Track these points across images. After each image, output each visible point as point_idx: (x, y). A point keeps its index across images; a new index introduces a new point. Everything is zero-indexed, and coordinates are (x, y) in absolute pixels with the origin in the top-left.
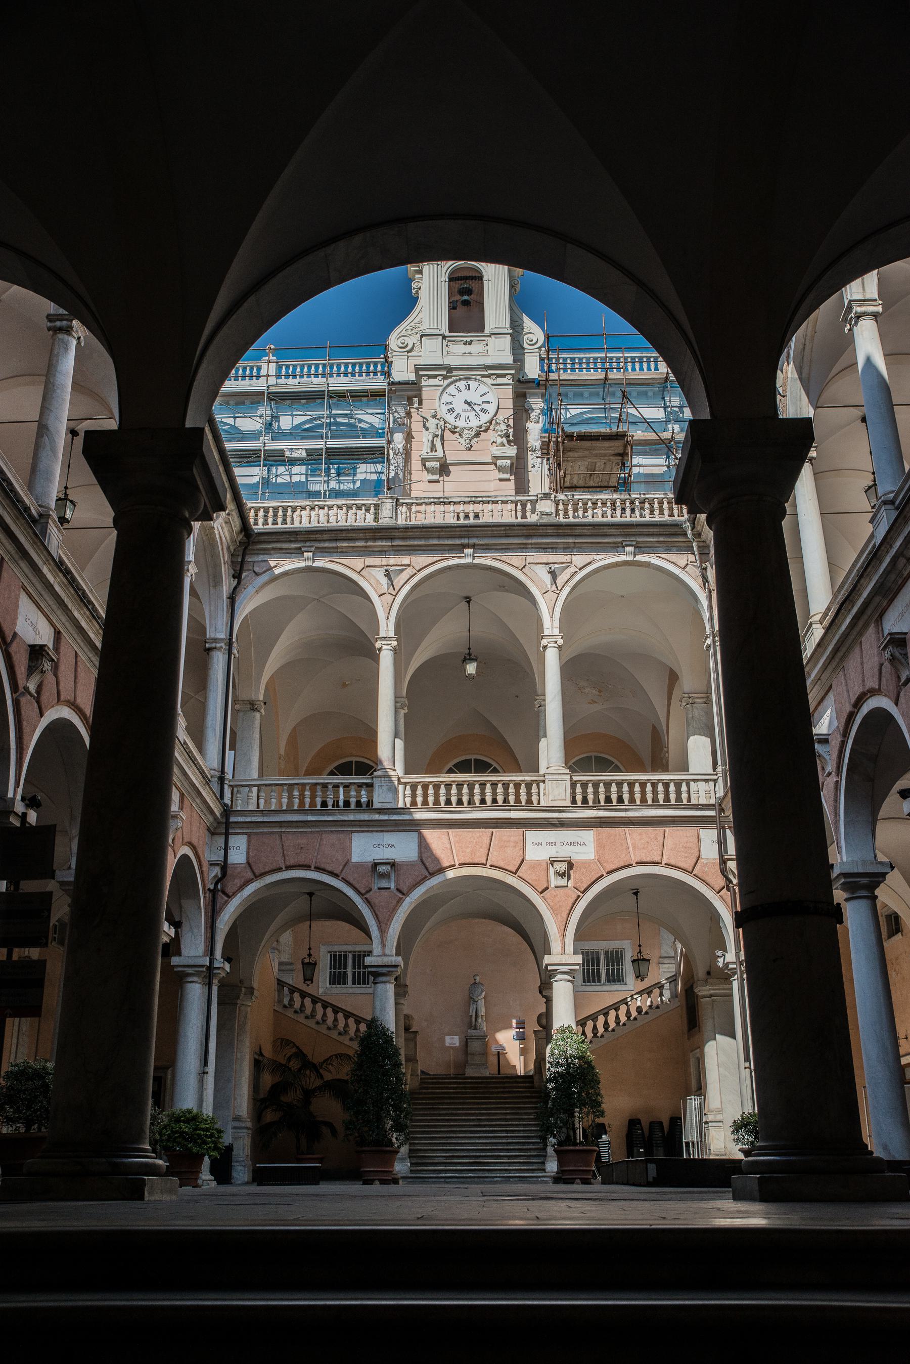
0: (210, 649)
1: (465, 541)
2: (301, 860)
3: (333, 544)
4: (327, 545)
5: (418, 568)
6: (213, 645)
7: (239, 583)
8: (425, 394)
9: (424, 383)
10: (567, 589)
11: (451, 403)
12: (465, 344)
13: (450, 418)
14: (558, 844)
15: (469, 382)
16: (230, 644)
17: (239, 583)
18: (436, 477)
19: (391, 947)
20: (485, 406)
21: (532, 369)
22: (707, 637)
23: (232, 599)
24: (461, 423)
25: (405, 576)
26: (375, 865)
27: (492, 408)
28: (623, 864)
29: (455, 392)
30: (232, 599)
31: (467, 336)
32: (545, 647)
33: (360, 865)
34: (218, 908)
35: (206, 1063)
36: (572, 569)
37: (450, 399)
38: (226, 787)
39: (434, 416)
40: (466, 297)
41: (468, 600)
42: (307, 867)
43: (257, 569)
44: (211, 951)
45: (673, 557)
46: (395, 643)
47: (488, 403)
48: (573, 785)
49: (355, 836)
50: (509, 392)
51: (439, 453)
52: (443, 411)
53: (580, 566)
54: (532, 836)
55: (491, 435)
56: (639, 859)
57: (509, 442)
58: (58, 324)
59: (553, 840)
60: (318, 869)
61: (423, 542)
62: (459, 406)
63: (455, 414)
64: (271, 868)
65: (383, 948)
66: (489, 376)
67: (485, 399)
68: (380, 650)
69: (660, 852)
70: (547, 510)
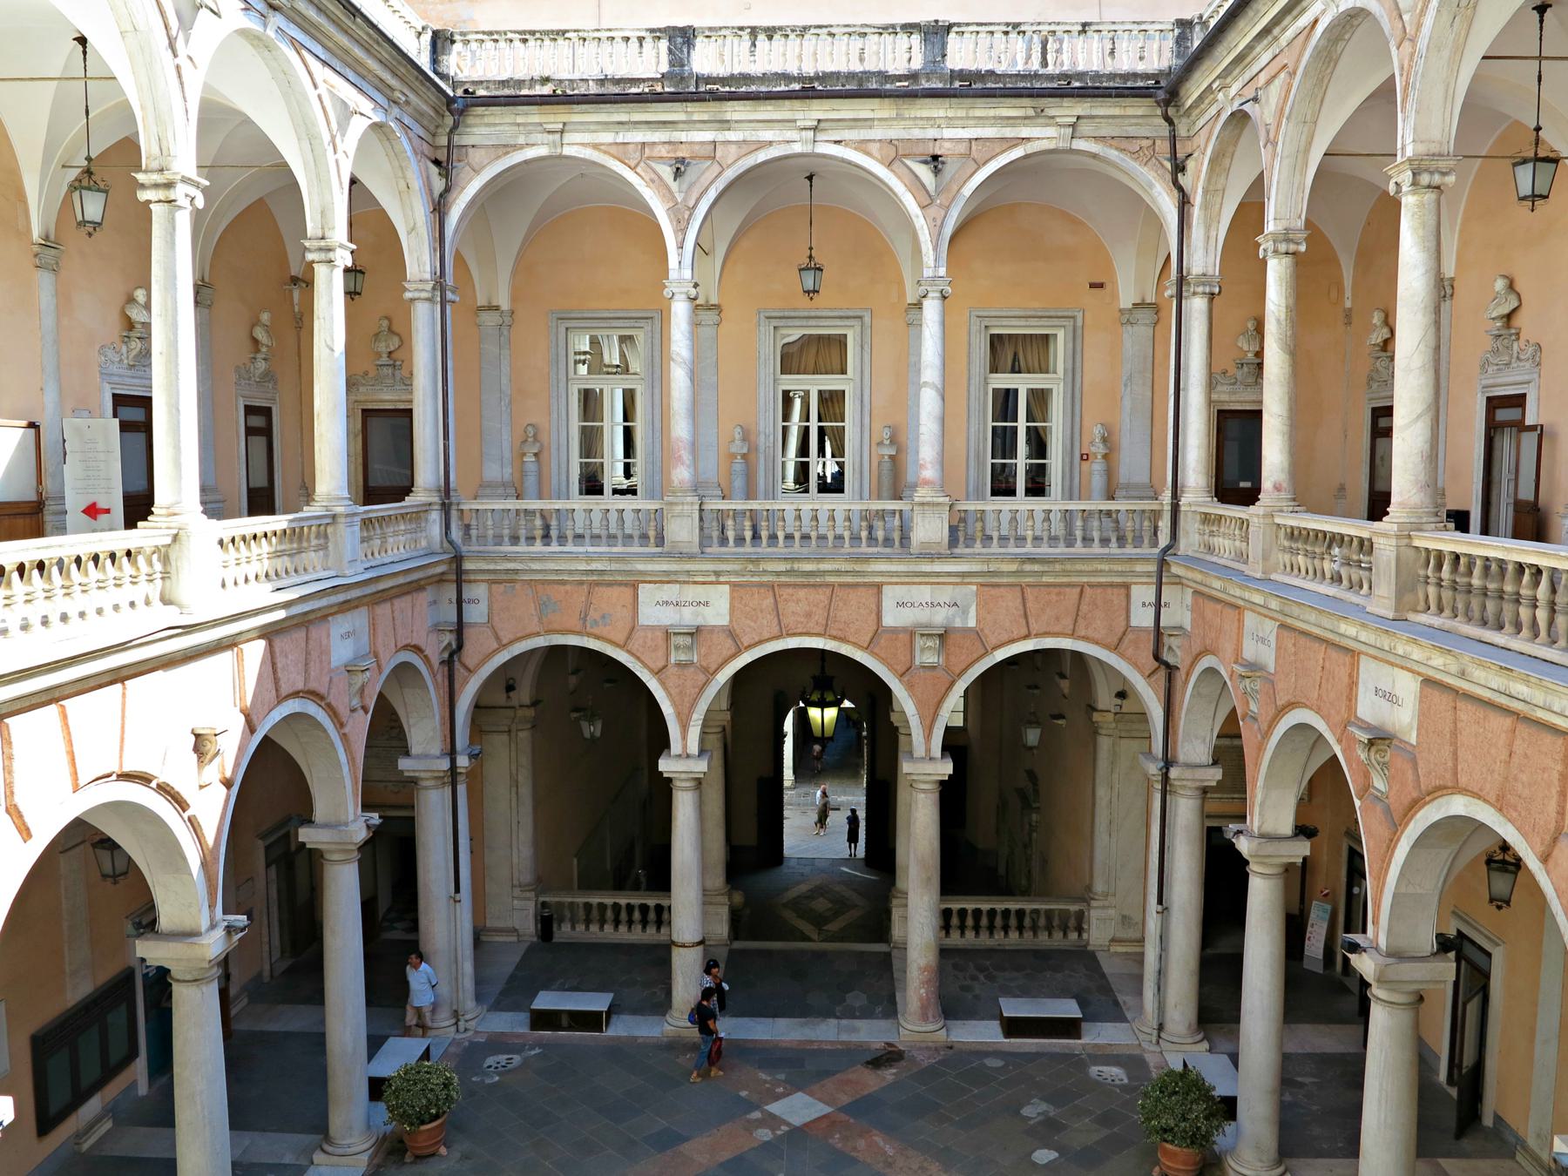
0: (412, 300)
6: (417, 295)
7: (447, 190)
17: (447, 190)
19: (693, 747)
23: (439, 208)
26: (668, 635)
30: (439, 208)
34: (457, 686)
35: (457, 890)
44: (452, 753)
65: (685, 747)
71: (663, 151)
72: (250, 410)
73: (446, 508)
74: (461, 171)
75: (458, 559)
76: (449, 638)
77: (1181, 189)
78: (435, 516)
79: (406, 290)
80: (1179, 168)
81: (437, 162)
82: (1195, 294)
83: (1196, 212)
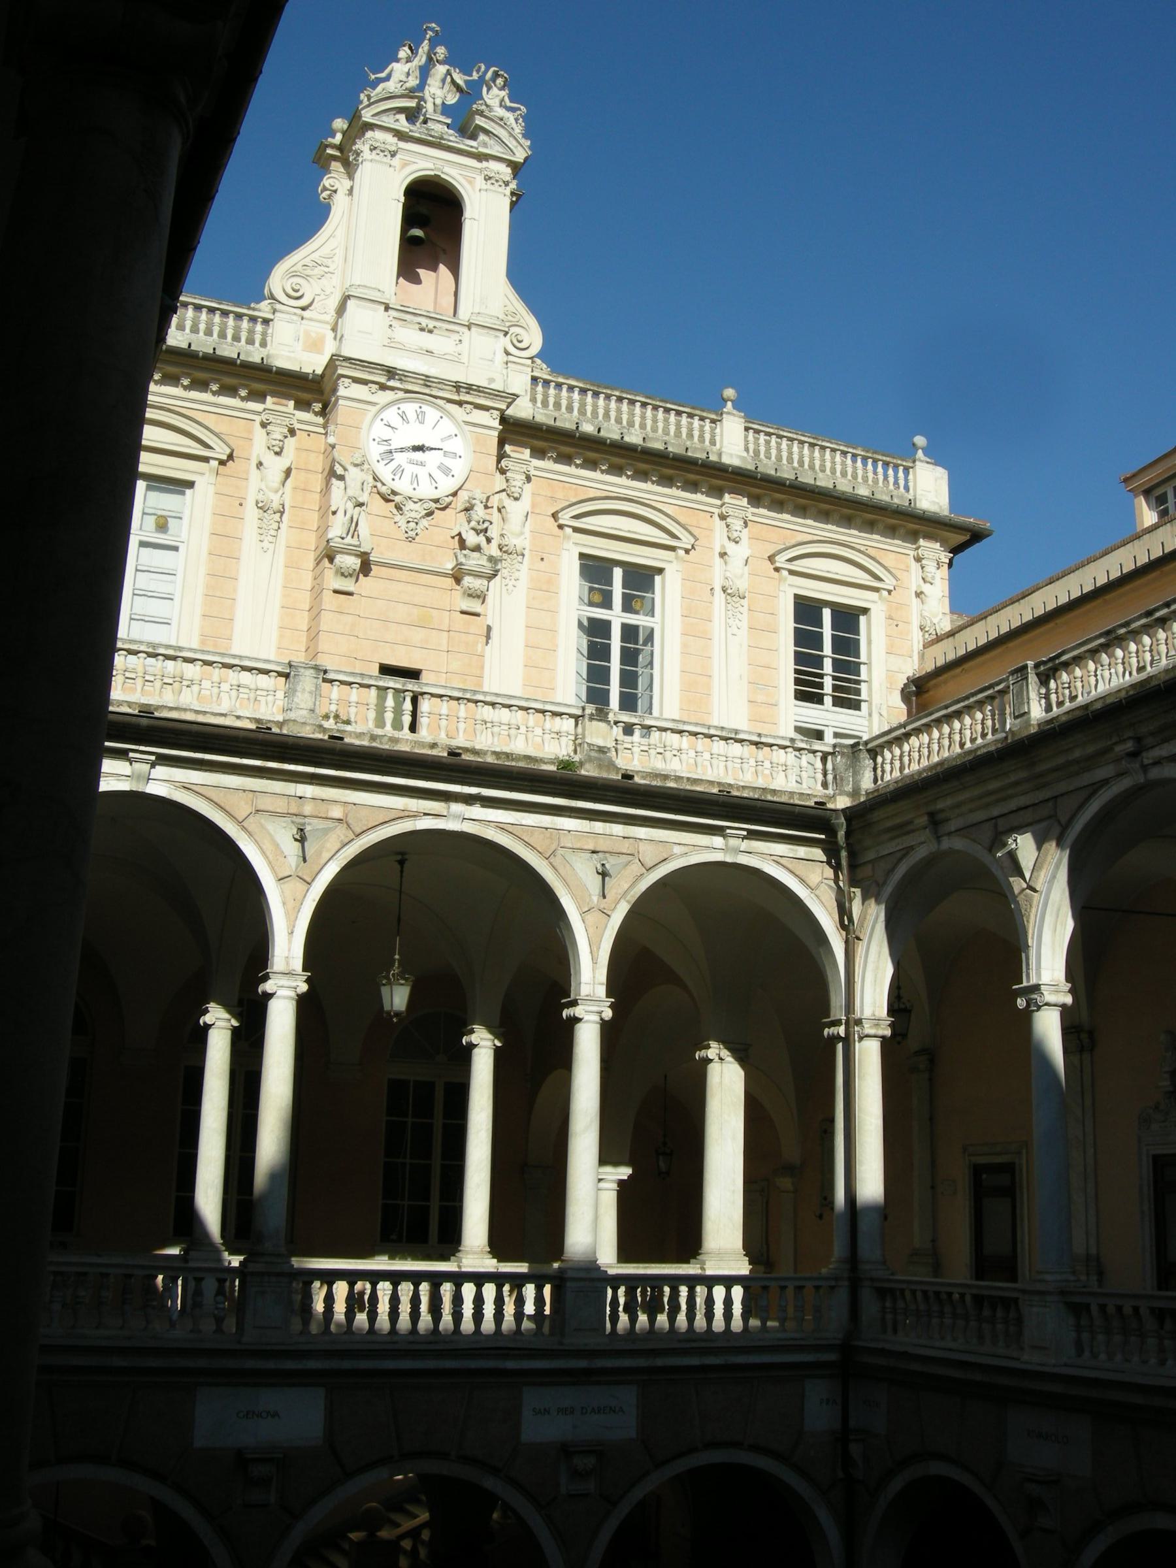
5: (358, 830)
9: (346, 390)
13: (385, 472)
15: (425, 408)
20: (449, 462)
22: (837, 1023)
24: (403, 486)
25: (332, 843)
27: (460, 468)
29: (396, 421)
37: (387, 433)
40: (417, 232)
45: (800, 867)
46: (304, 987)
52: (374, 451)
53: (649, 864)
54: (532, 1398)
63: (393, 465)
66: (460, 403)
70: (601, 744)
71: (280, 805)
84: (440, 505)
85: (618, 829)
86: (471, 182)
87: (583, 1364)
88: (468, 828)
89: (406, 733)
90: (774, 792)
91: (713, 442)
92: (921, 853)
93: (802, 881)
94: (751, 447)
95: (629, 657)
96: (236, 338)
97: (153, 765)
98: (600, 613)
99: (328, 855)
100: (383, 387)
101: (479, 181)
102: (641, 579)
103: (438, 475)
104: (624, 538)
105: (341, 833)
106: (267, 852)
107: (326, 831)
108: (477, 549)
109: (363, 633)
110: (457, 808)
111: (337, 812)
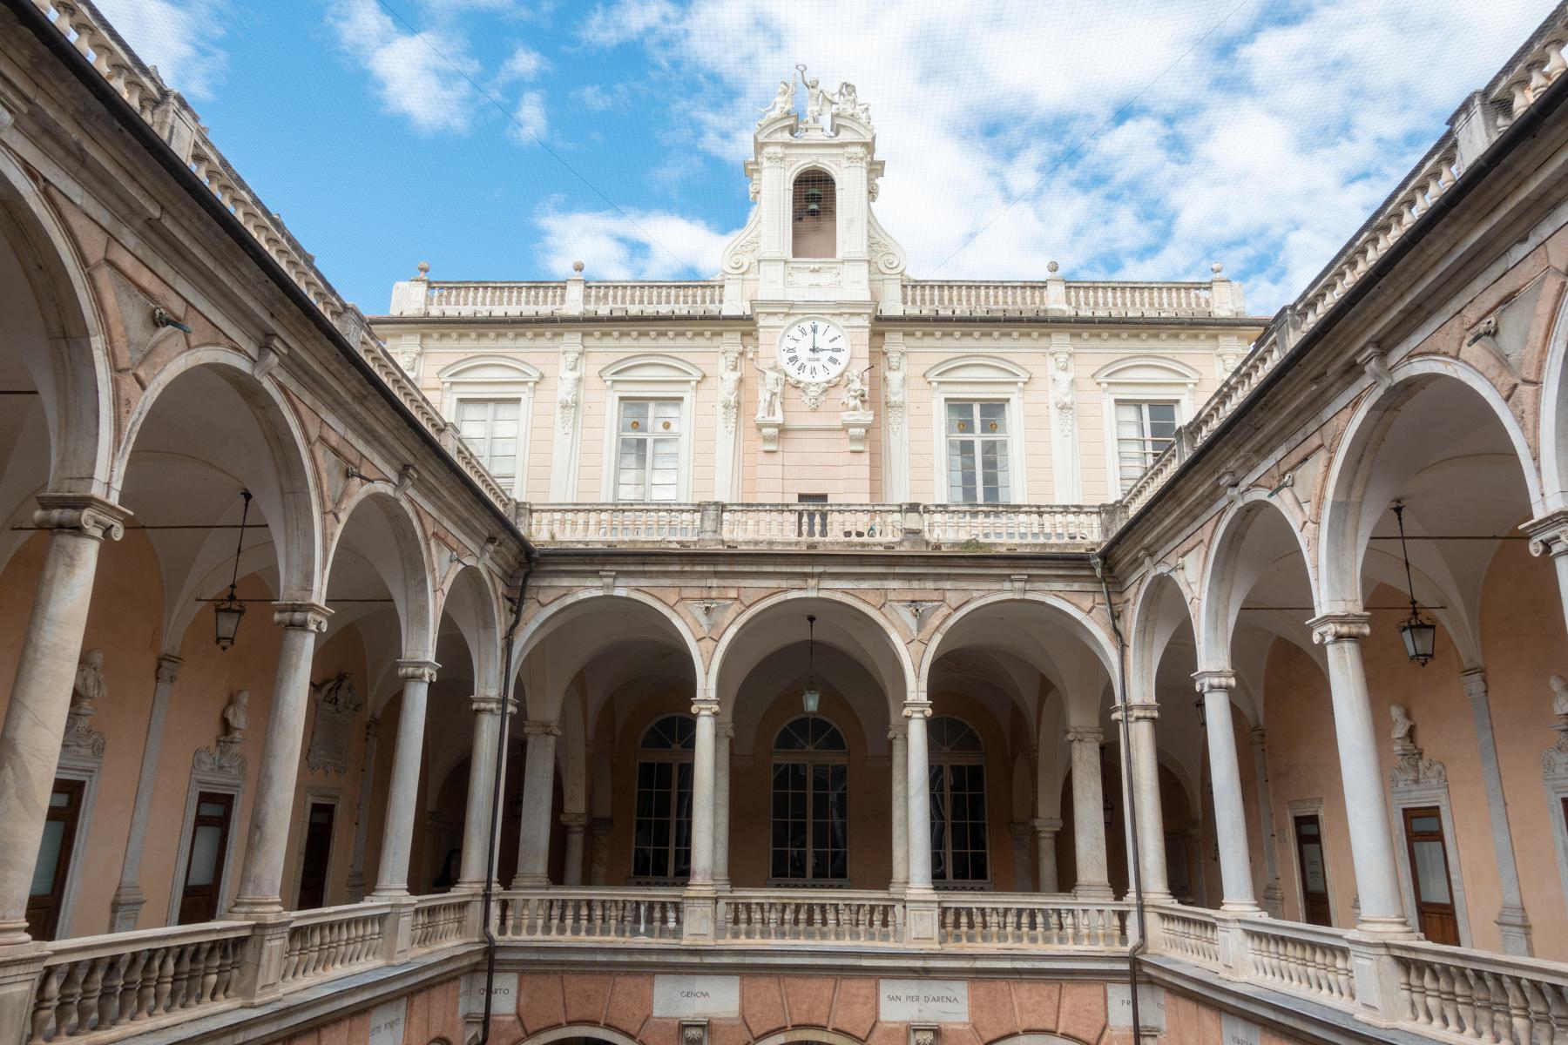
0: (478, 711)
1: (808, 569)
2: (588, 1012)
3: (640, 568)
4: (632, 568)
6: (483, 705)
7: (517, 622)
8: (762, 334)
9: (761, 323)
10: (938, 638)
11: (793, 350)
12: (814, 271)
13: (792, 370)
14: (922, 999)
16: (503, 701)
18: (772, 447)
20: (835, 355)
21: (893, 306)
22: (1116, 710)
24: (805, 377)
25: (731, 614)
26: (683, 1027)
27: (843, 358)
28: (1005, 1032)
31: (812, 262)
32: (908, 718)
33: (663, 1023)
36: (945, 610)
37: (792, 344)
38: (493, 905)
39: (774, 368)
40: (814, 206)
41: (811, 619)
42: (595, 1023)
43: (542, 599)
45: (1075, 598)
47: (839, 350)
48: (944, 911)
49: (659, 980)
50: (866, 334)
51: (778, 418)
54: (887, 988)
55: (843, 395)
56: (1026, 1026)
57: (863, 402)
58: (56, 514)
59: (914, 992)
60: (608, 1026)
61: (754, 569)
62: (804, 353)
64: (549, 1023)
67: (835, 345)
68: (696, 716)
69: (1054, 1017)
70: (914, 526)
71: (696, 593)
72: (315, 807)
73: (487, 898)
74: (529, 609)
75: (490, 950)
76: (477, 1029)
77: (1117, 632)
78: (476, 911)
79: (472, 702)
80: (1116, 616)
81: (510, 600)
82: (1138, 719)
83: (1130, 652)
84: (832, 386)
85: (930, 585)
86: (838, 165)
87: (919, 964)
88: (823, 594)
89: (805, 537)
90: (1052, 546)
91: (1042, 302)
92: (1148, 579)
93: (1077, 607)
94: (1073, 300)
95: (990, 464)
96: (704, 302)
97: (615, 578)
98: (966, 437)
99: (727, 622)
100: (787, 314)
101: (845, 163)
102: (994, 410)
103: (830, 365)
104: (977, 383)
105: (737, 607)
106: (688, 624)
107: (727, 607)
108: (855, 409)
109: (781, 480)
110: (812, 582)
111: (733, 594)
